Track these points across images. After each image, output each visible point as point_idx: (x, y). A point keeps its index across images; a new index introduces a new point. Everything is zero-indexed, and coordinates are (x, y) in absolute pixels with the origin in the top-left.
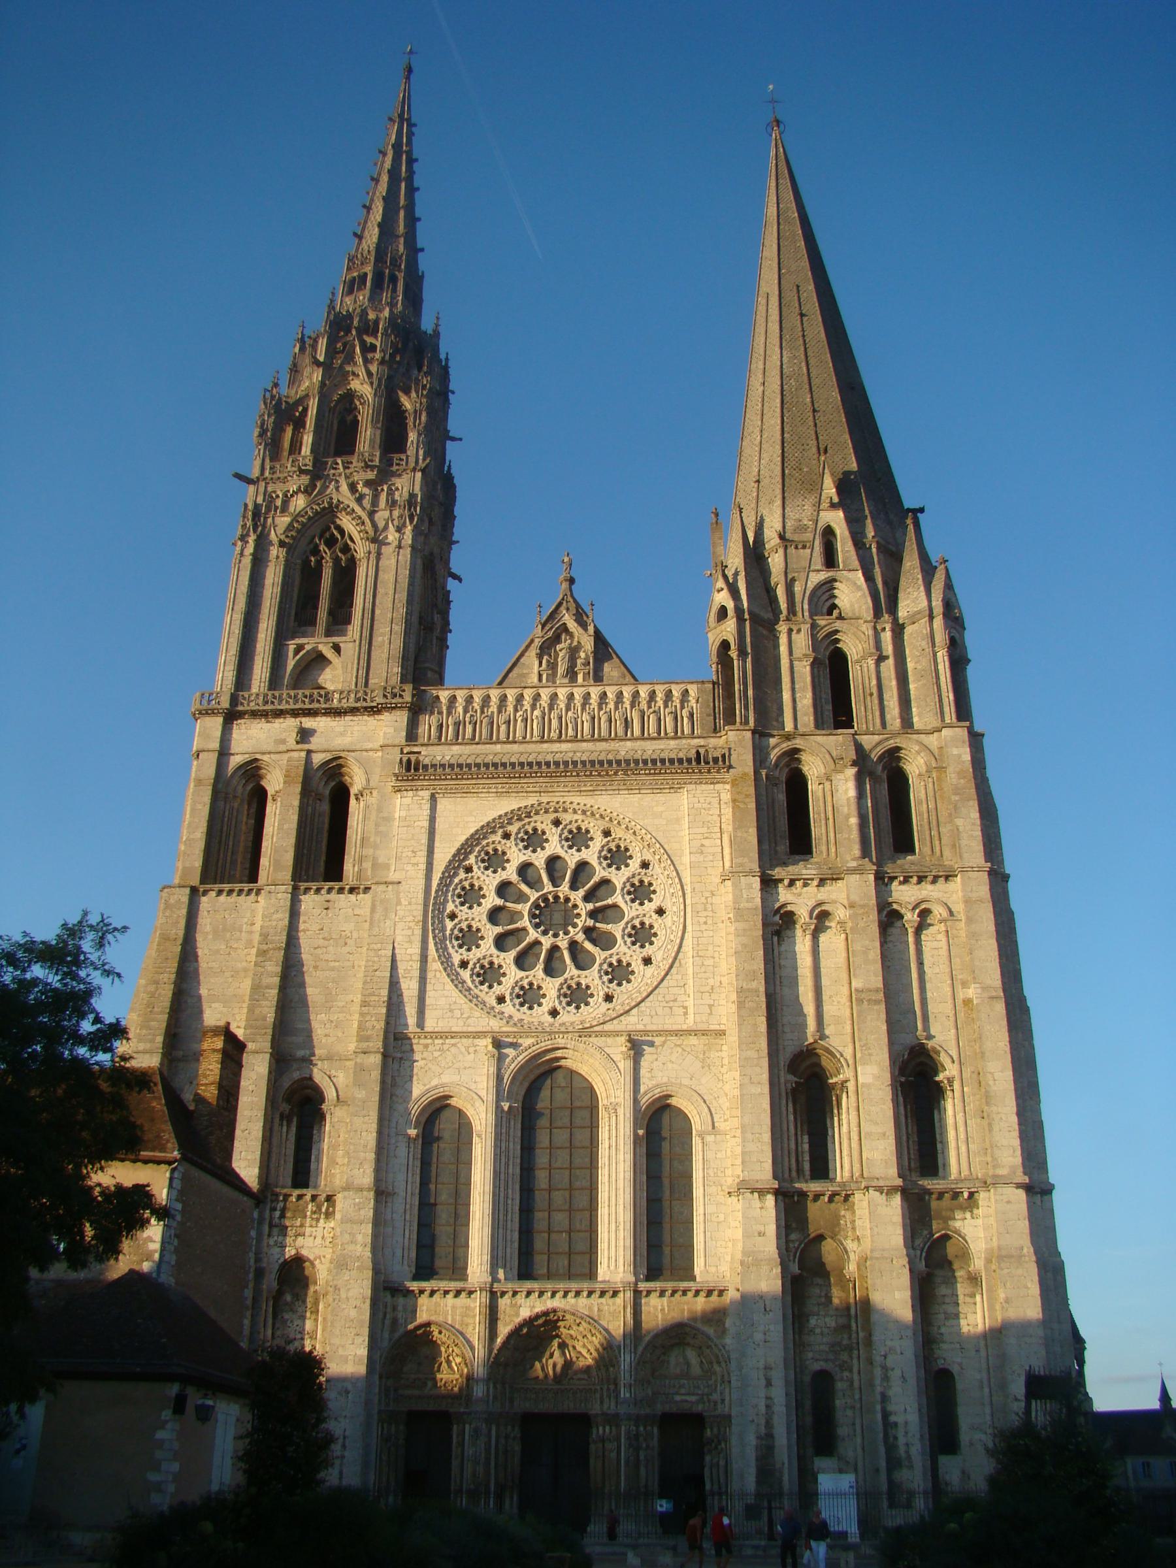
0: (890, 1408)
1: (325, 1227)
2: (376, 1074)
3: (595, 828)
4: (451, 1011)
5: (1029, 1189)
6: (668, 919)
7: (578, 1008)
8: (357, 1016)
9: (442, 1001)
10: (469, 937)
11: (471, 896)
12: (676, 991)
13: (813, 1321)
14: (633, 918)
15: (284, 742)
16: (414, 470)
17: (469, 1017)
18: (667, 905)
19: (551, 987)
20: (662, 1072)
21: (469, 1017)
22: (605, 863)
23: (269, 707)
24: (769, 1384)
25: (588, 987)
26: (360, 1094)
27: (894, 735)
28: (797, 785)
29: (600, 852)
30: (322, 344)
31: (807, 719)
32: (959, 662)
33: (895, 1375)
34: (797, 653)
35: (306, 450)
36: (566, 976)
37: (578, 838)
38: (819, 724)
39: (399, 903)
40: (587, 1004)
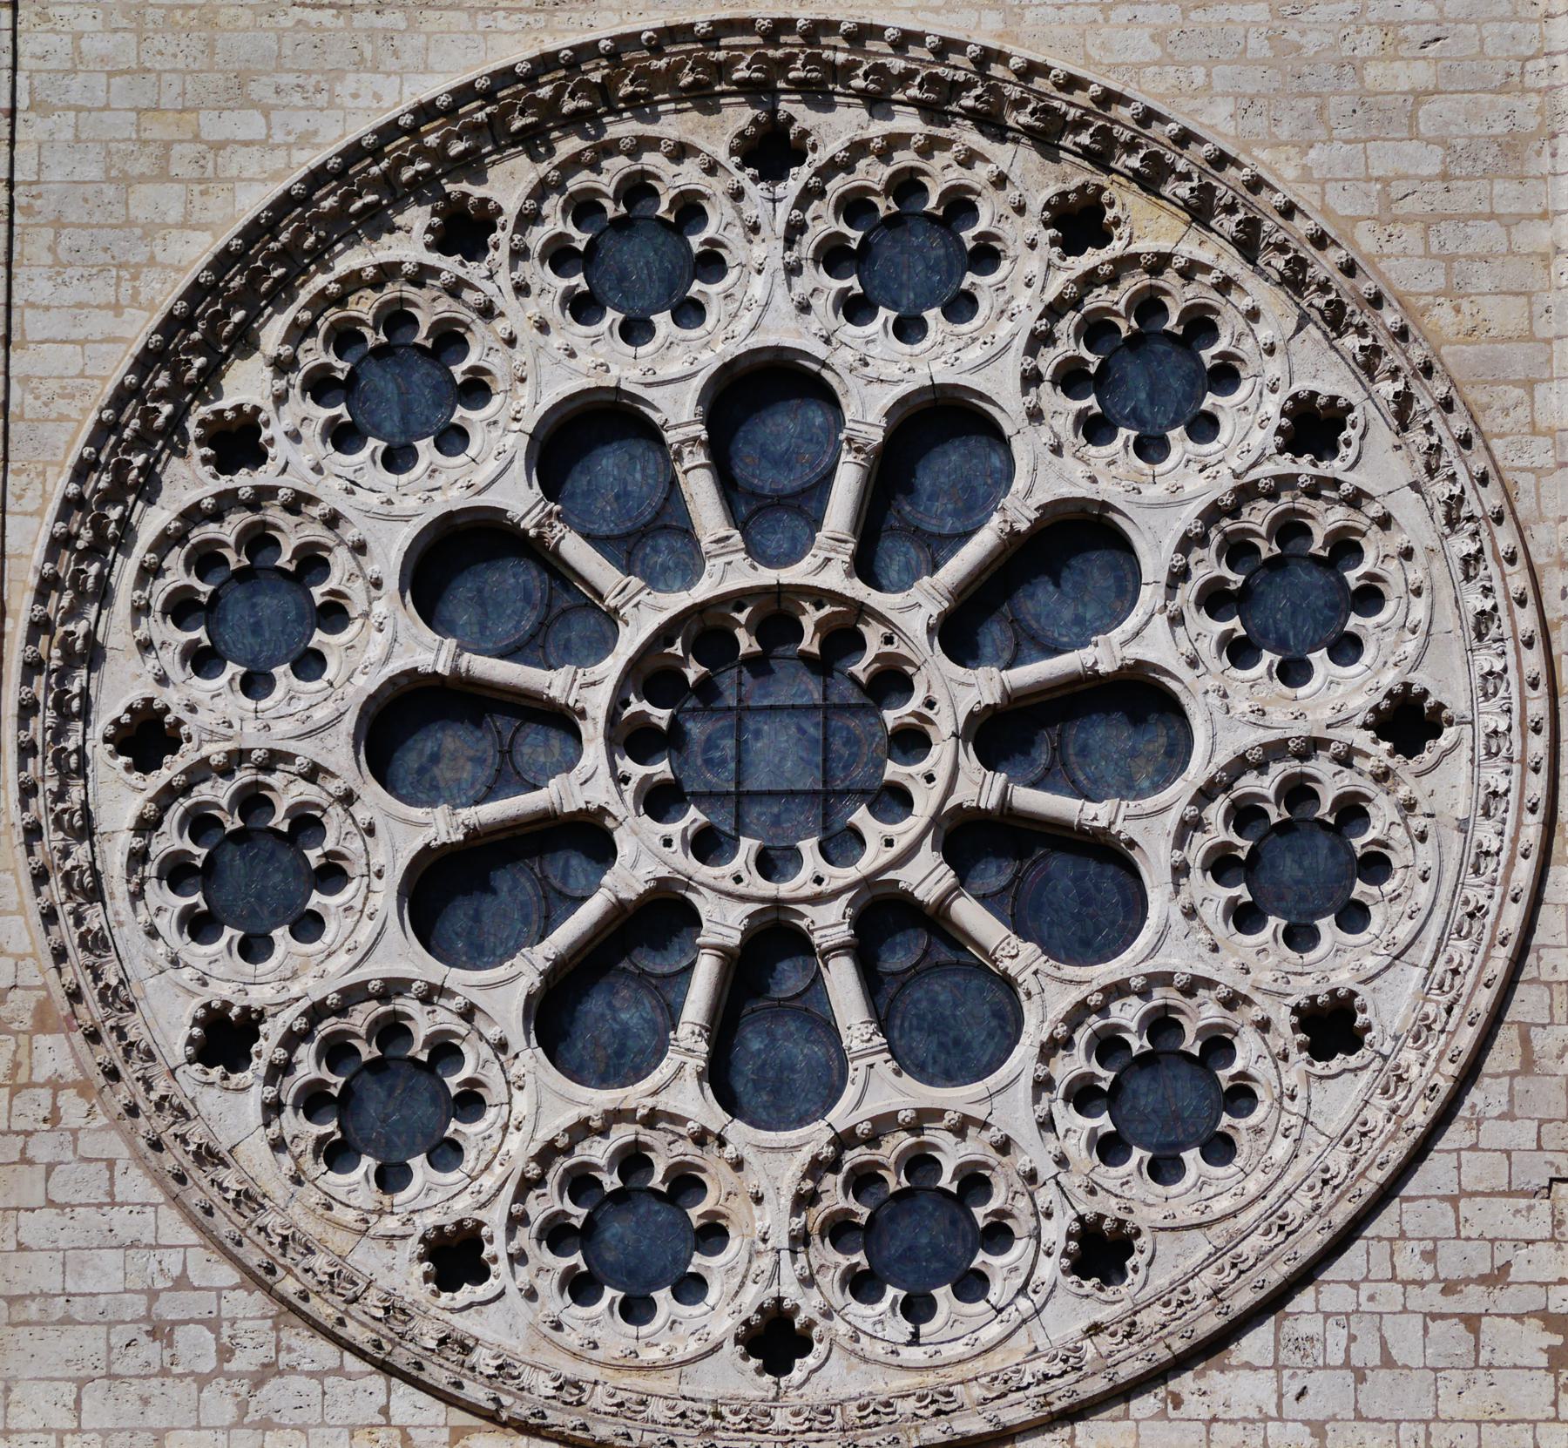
3: (1015, 186)
4: (160, 1332)
6: (1448, 778)
7: (917, 1309)
9: (106, 1274)
11: (257, 602)
12: (1498, 1216)
14: (1241, 765)
17: (269, 1370)
18: (1447, 683)
19: (761, 1176)
21: (269, 1370)
22: (1063, 409)
25: (975, 1182)
29: (1039, 340)
36: (842, 1115)
40: (972, 1286)
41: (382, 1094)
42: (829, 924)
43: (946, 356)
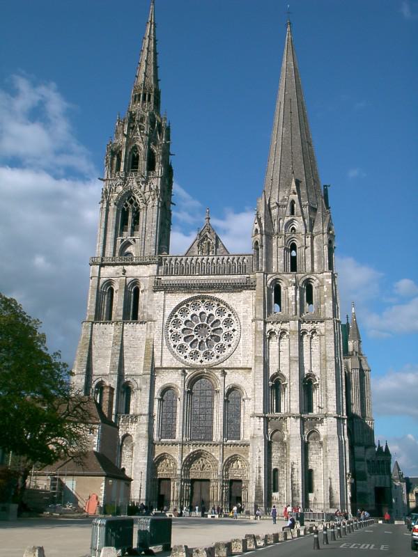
0: (294, 479)
1: (134, 425)
2: (149, 381)
5: (338, 418)
8: (143, 363)
10: (176, 337)
11: (177, 323)
13: (274, 454)
15: (118, 274)
16: (158, 177)
18: (236, 329)
20: (233, 378)
23: (114, 262)
24: (260, 472)
26: (144, 387)
27: (308, 274)
28: (278, 290)
30: (126, 126)
31: (281, 268)
32: (331, 251)
33: (296, 470)
34: (280, 245)
35: (122, 169)
37: (209, 306)
38: (285, 271)
39: (155, 327)
41: (182, 348)
42: (205, 341)
43: (211, 312)
